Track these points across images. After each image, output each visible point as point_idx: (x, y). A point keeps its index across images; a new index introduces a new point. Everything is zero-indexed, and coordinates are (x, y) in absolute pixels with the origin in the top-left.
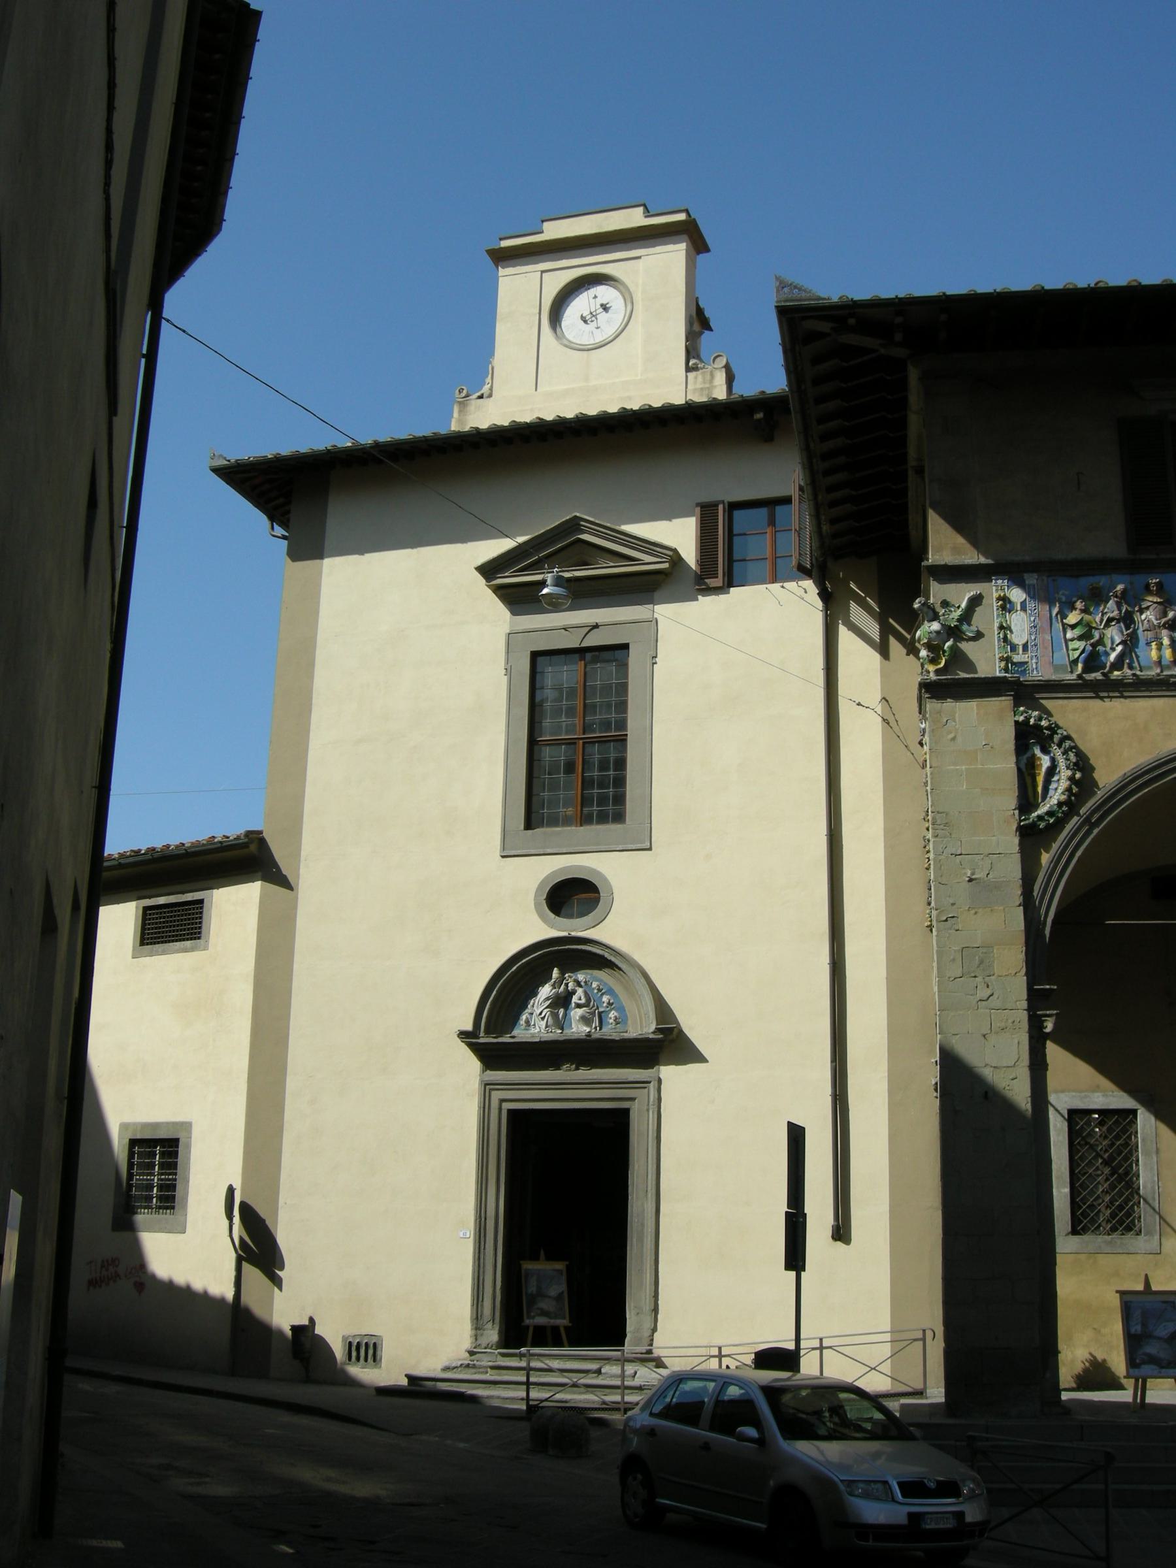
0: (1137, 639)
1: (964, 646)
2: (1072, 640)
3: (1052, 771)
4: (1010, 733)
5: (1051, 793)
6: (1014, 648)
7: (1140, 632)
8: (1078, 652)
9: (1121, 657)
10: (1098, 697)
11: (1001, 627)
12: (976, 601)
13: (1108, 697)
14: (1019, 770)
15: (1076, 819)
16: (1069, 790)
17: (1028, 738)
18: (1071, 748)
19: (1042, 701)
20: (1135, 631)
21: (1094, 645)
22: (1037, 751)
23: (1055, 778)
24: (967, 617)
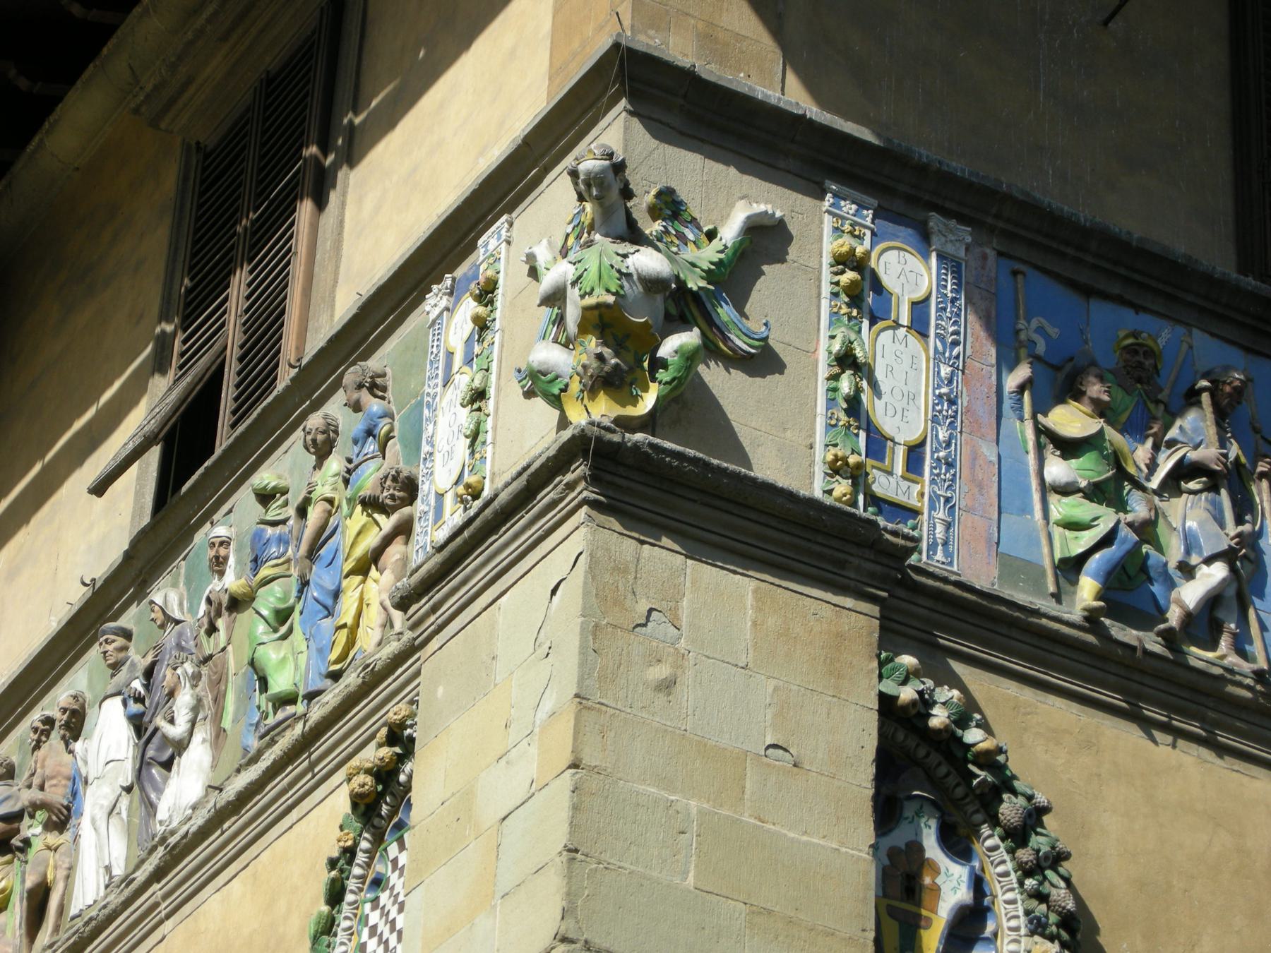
1: (714, 376)
6: (878, 444)
8: (1086, 540)
11: (845, 360)
13: (1166, 728)
19: (958, 667)
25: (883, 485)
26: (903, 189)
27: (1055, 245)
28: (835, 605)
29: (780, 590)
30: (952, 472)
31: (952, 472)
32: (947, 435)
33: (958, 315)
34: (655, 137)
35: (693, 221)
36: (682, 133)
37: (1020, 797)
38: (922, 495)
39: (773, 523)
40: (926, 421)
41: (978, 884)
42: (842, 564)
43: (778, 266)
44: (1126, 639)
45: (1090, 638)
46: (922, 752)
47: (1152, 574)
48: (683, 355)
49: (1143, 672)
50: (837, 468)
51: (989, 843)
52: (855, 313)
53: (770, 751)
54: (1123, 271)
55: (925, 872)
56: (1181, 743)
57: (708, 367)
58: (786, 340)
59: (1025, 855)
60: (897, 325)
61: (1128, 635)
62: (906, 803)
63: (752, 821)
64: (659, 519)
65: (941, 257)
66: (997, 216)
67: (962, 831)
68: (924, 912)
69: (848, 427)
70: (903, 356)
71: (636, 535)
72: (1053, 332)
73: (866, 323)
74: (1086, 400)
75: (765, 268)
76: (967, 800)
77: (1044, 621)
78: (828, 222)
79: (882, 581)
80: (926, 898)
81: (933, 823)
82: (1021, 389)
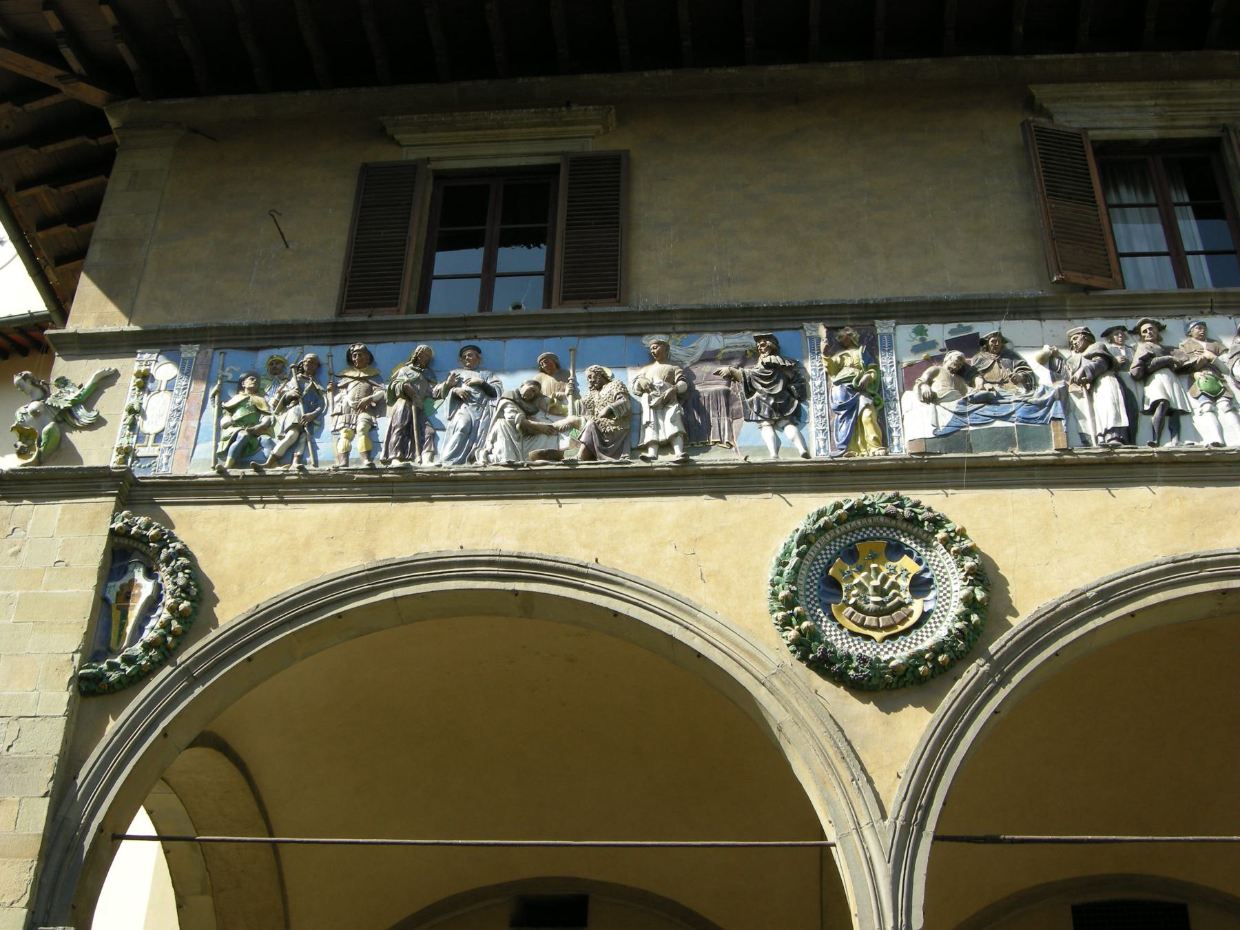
0: (322, 426)
1: (75, 437)
2: (226, 427)
4: (99, 543)
6: (141, 438)
7: (327, 418)
9: (291, 448)
10: (246, 502)
12: (108, 379)
15: (168, 669)
17: (123, 553)
18: (184, 567)
19: (164, 508)
20: (320, 416)
21: (254, 435)
24: (89, 398)
25: (141, 452)
41: (159, 588)
82: (214, 396)
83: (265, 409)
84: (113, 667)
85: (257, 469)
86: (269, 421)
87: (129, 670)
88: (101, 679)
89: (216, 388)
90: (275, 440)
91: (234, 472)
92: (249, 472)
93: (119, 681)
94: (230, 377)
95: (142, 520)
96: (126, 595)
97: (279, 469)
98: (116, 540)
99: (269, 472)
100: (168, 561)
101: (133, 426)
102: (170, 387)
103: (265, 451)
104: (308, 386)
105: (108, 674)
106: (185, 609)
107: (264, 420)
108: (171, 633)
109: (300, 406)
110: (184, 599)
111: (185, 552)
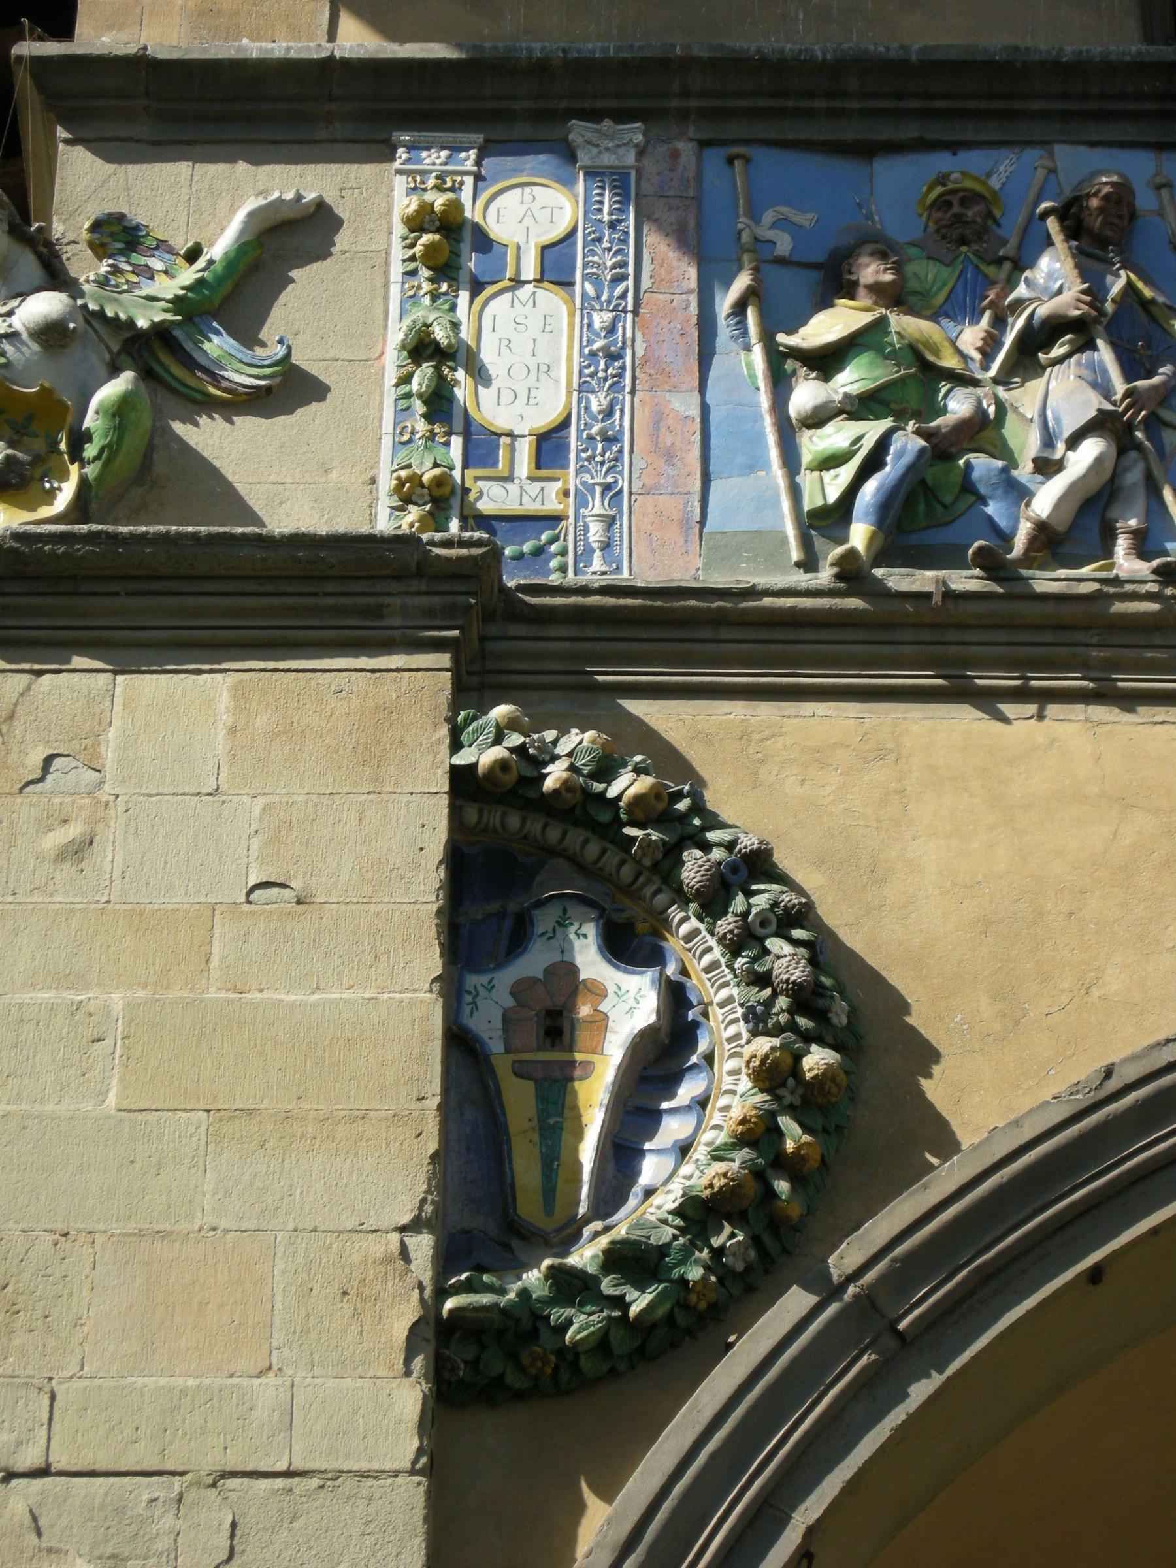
1: (207, 436)
2: (817, 419)
3: (666, 1052)
4: (417, 831)
5: (650, 1170)
6: (482, 446)
8: (847, 472)
10: (959, 692)
11: (422, 348)
13: (1020, 695)
14: (460, 1043)
15: (795, 1302)
16: (757, 1135)
17: (525, 869)
19: (637, 707)
21: (943, 448)
22: (589, 958)
23: (688, 1090)
25: (493, 498)
26: (506, 102)
27: (790, 104)
28: (373, 671)
29: (276, 675)
30: (615, 448)
31: (615, 448)
32: (605, 403)
33: (625, 241)
34: (109, 159)
35: (162, 246)
36: (154, 143)
37: (715, 850)
38: (566, 493)
39: (249, 587)
40: (569, 393)
41: (675, 996)
42: (377, 612)
43: (315, 267)
44: (916, 587)
45: (853, 603)
46: (553, 835)
47: (983, 490)
48: (106, 413)
49: (962, 626)
50: (408, 492)
51: (684, 929)
52: (444, 287)
53: (258, 893)
54: (914, 104)
55: (579, 1001)
56: (1052, 709)
57: (197, 425)
58: (330, 356)
59: (725, 925)
60: (517, 283)
61: (923, 580)
62: (536, 912)
63: (223, 995)
64: (60, 634)
65: (590, 174)
66: (685, 94)
67: (642, 927)
68: (579, 1057)
69: (432, 436)
70: (529, 322)
71: (27, 666)
72: (805, 219)
73: (464, 296)
74: (862, 292)
75: (294, 274)
76: (641, 880)
77: (767, 601)
78: (401, 184)
79: (447, 615)
80: (583, 1037)
81: (590, 929)
82: (740, 308)
83: (949, 361)
84: (571, 1286)
85: (992, 563)
86: (980, 412)
87: (639, 1302)
88: (533, 1335)
89: (742, 282)
90: (1024, 472)
91: (899, 579)
92: (967, 580)
93: (601, 1344)
94: (784, 245)
95: (577, 741)
96: (555, 1020)
97: (1084, 577)
98: (471, 814)
99: (1047, 581)
100: (712, 902)
101: (439, 404)
102: (556, 265)
103: (991, 509)
104: (1117, 286)
105: (557, 1314)
106: (827, 1076)
107: (959, 405)
108: (781, 1163)
109: (1104, 353)
110: (808, 1038)
111: (758, 865)
